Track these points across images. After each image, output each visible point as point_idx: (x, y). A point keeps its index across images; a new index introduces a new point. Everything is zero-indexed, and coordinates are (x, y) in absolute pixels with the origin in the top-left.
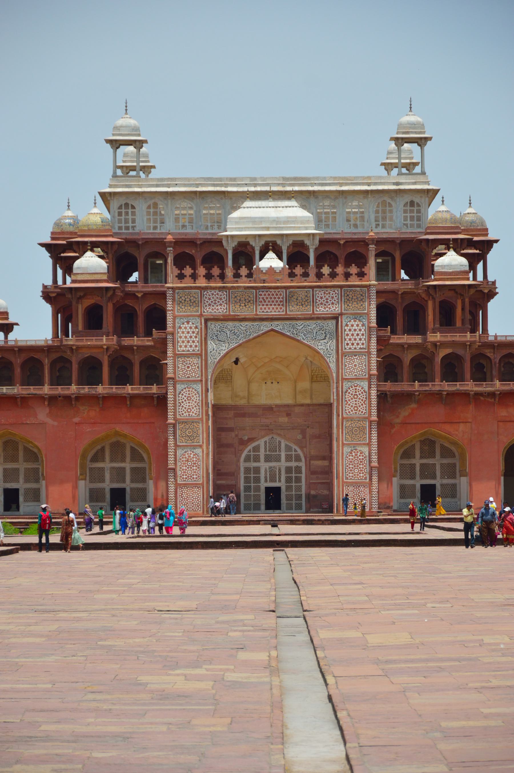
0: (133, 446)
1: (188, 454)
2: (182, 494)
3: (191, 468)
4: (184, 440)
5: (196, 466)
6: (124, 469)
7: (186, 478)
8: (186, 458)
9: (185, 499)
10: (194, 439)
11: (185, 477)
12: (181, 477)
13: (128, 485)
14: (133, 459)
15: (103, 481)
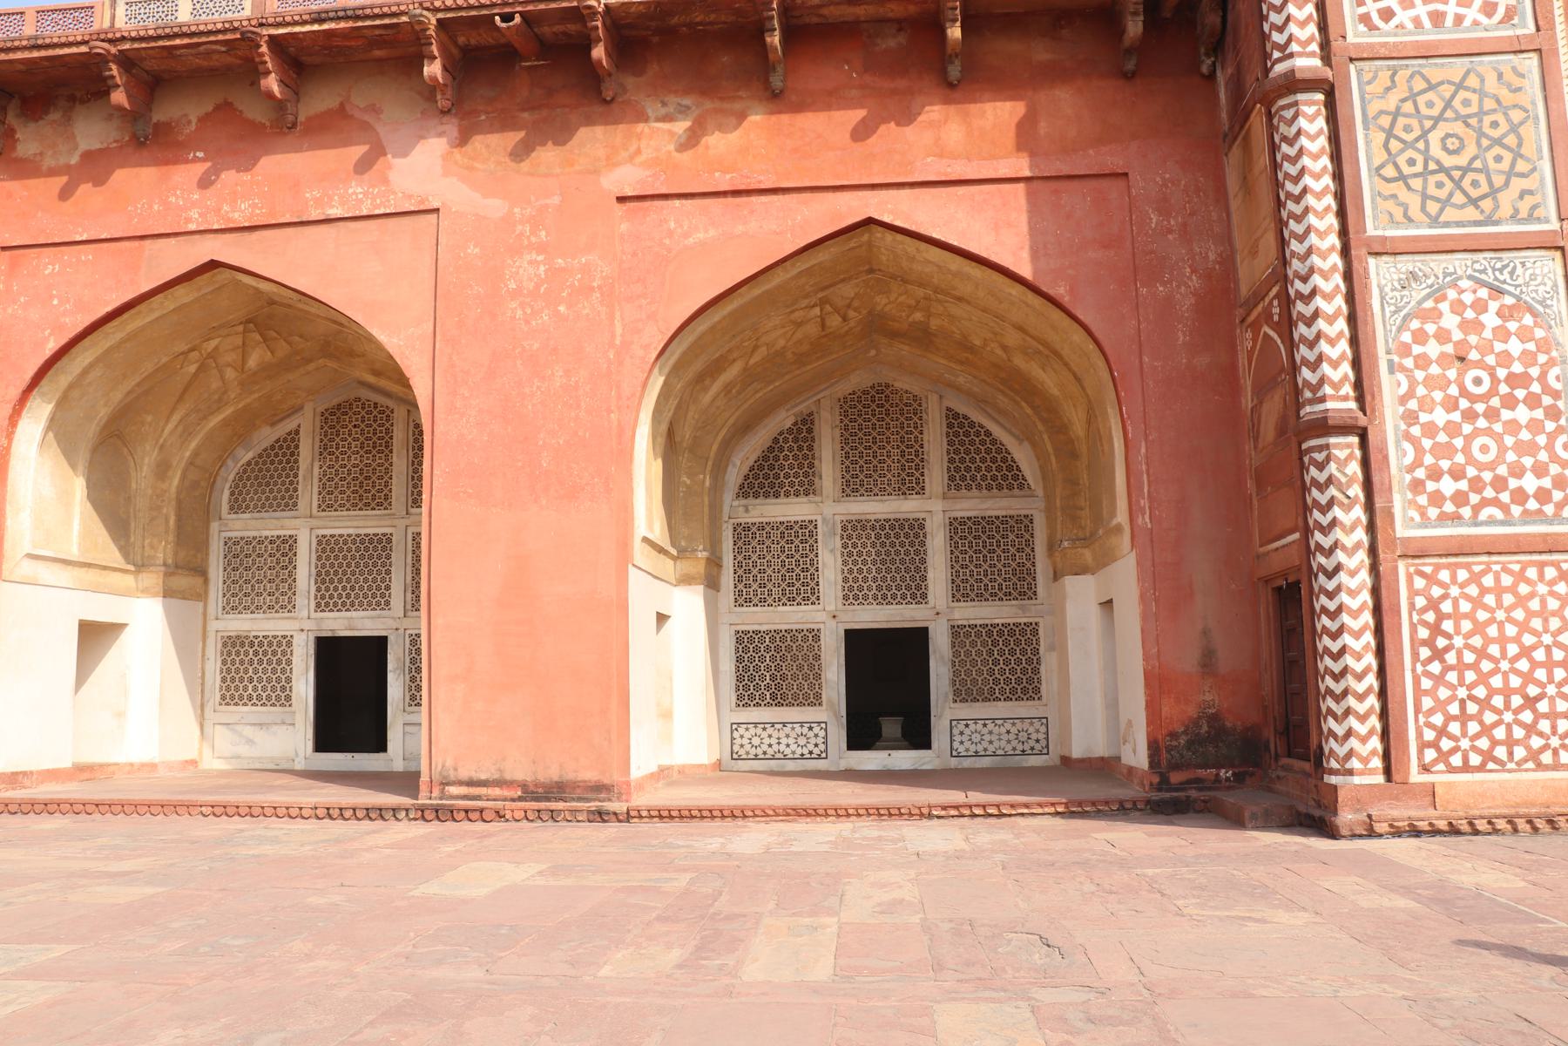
0: (962, 409)
1: (1459, 307)
2: (1436, 629)
3: (1492, 414)
4: (1414, 202)
5: (1533, 402)
6: (913, 530)
7: (1460, 499)
8: (1443, 336)
9: (1461, 667)
10: (1493, 192)
11: (1448, 486)
12: (1417, 486)
13: (939, 611)
14: (959, 480)
15: (808, 593)
